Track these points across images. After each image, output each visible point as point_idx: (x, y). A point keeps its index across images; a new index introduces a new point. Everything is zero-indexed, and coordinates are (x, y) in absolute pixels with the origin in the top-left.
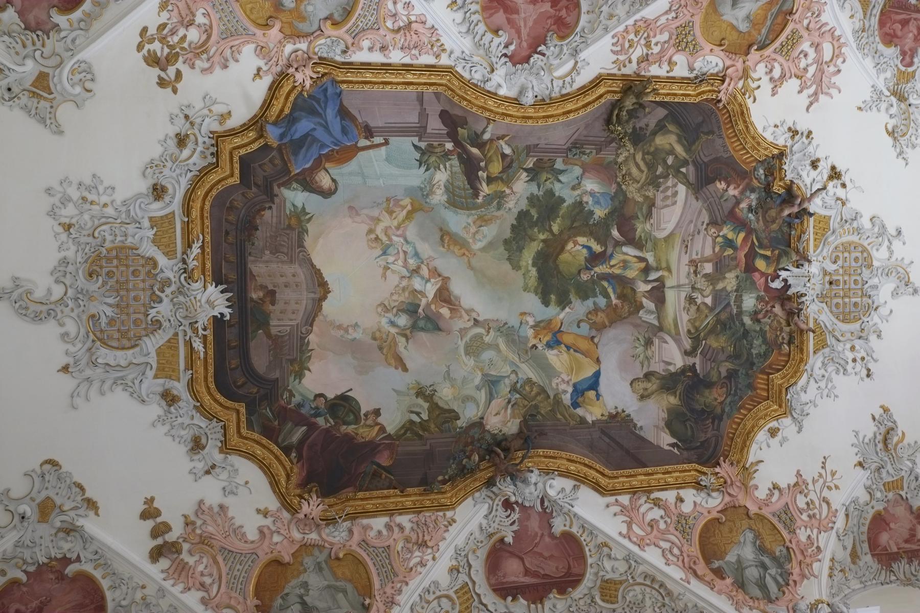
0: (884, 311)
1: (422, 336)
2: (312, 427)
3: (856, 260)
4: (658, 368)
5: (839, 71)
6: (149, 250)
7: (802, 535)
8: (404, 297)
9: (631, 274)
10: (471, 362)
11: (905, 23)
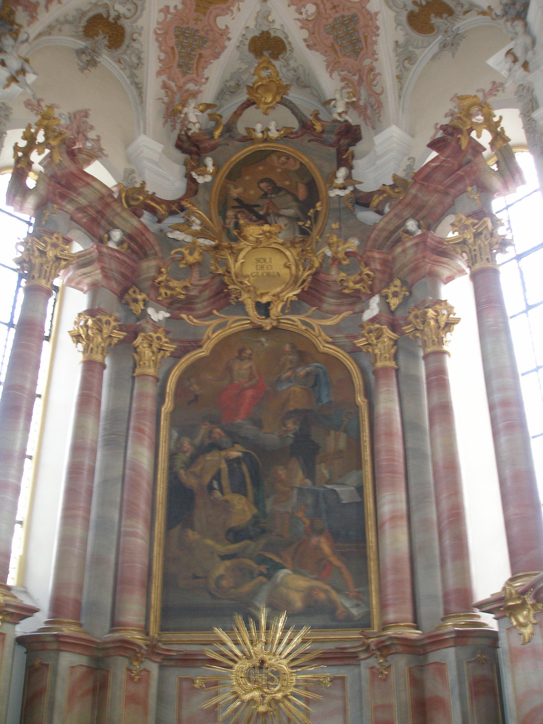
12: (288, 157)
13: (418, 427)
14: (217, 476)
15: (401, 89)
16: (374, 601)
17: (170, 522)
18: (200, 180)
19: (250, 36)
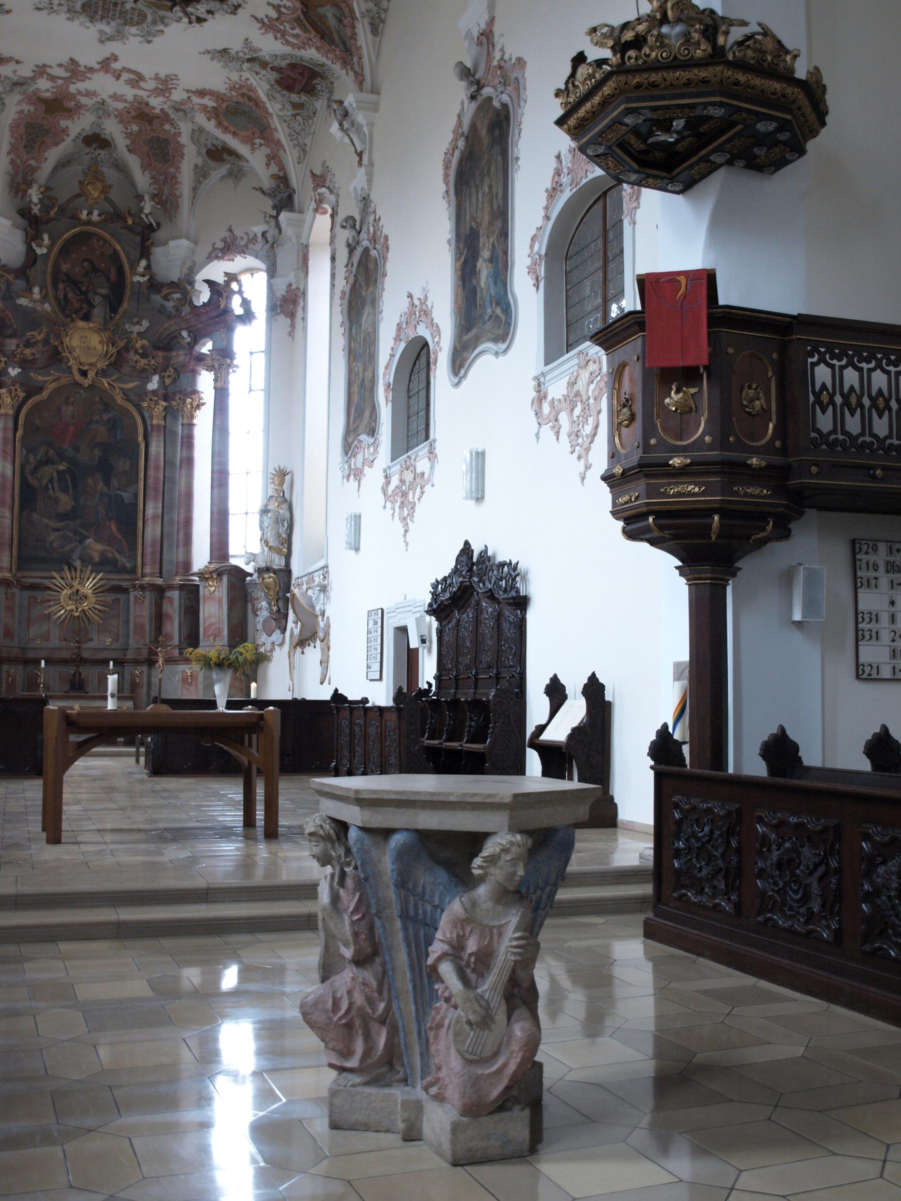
0: (89, 24)
3: (132, 19)
5: (276, 39)
11: (302, 74)
12: (105, 241)
13: (173, 465)
14: (51, 481)
15: (194, 198)
16: (139, 560)
17: (22, 508)
18: (40, 251)
19: (84, 134)
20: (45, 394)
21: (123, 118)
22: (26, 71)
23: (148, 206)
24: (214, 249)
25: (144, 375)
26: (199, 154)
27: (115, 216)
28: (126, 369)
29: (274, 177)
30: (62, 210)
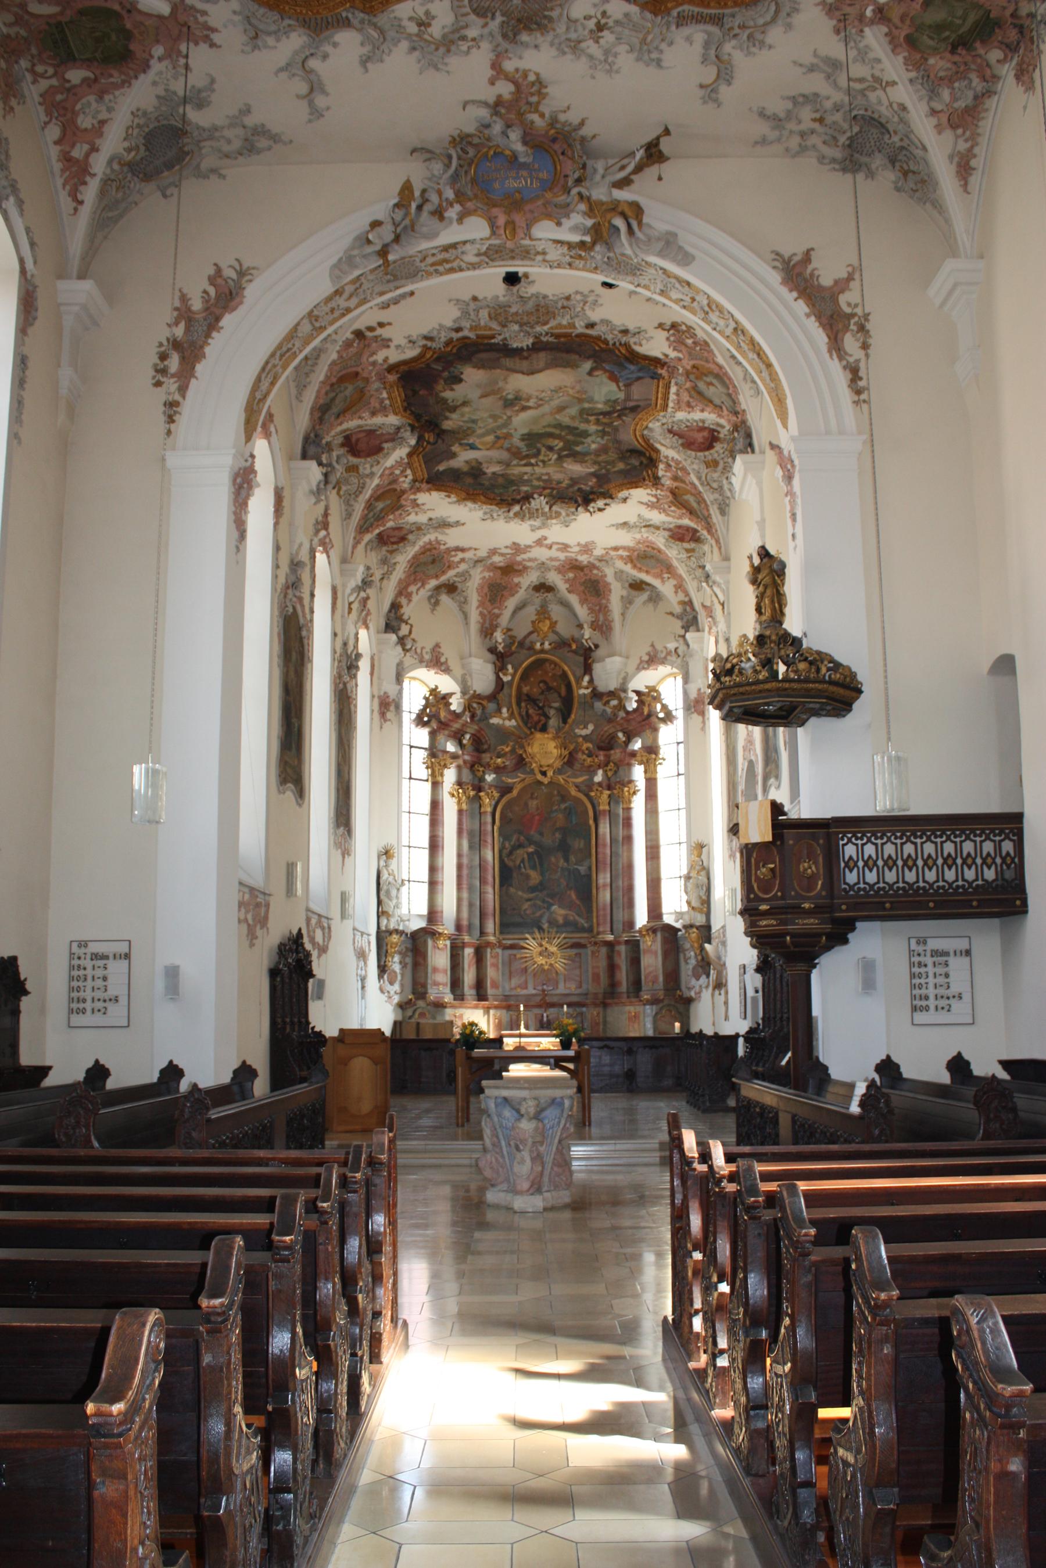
1: (501, 403)
2: (443, 371)
4: (485, 465)
6: (553, 323)
7: (391, 517)
8: (524, 396)
9: (541, 457)
10: (486, 415)
12: (556, 664)
13: (617, 841)
14: (523, 861)
16: (595, 920)
17: (501, 885)
18: (506, 679)
20: (515, 792)
21: (560, 570)
22: (483, 553)
23: (587, 633)
24: (641, 661)
25: (591, 771)
26: (623, 587)
27: (562, 644)
28: (577, 766)
29: (682, 603)
30: (521, 644)
